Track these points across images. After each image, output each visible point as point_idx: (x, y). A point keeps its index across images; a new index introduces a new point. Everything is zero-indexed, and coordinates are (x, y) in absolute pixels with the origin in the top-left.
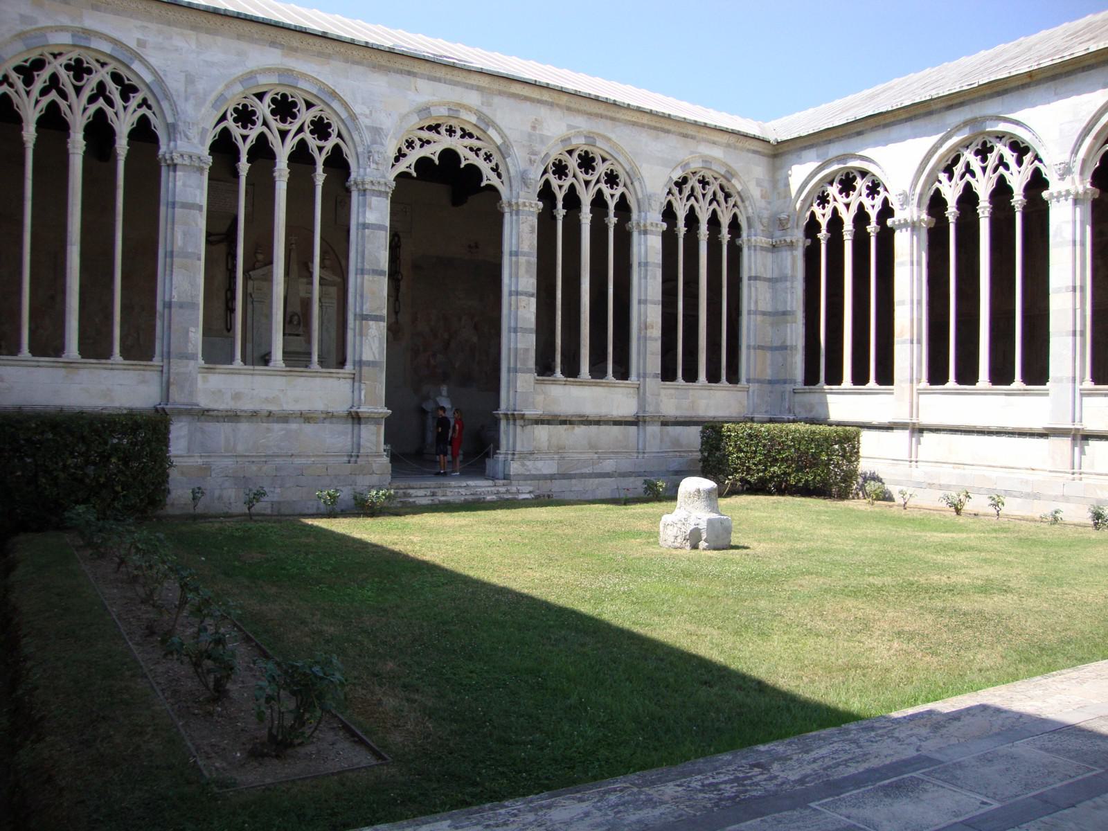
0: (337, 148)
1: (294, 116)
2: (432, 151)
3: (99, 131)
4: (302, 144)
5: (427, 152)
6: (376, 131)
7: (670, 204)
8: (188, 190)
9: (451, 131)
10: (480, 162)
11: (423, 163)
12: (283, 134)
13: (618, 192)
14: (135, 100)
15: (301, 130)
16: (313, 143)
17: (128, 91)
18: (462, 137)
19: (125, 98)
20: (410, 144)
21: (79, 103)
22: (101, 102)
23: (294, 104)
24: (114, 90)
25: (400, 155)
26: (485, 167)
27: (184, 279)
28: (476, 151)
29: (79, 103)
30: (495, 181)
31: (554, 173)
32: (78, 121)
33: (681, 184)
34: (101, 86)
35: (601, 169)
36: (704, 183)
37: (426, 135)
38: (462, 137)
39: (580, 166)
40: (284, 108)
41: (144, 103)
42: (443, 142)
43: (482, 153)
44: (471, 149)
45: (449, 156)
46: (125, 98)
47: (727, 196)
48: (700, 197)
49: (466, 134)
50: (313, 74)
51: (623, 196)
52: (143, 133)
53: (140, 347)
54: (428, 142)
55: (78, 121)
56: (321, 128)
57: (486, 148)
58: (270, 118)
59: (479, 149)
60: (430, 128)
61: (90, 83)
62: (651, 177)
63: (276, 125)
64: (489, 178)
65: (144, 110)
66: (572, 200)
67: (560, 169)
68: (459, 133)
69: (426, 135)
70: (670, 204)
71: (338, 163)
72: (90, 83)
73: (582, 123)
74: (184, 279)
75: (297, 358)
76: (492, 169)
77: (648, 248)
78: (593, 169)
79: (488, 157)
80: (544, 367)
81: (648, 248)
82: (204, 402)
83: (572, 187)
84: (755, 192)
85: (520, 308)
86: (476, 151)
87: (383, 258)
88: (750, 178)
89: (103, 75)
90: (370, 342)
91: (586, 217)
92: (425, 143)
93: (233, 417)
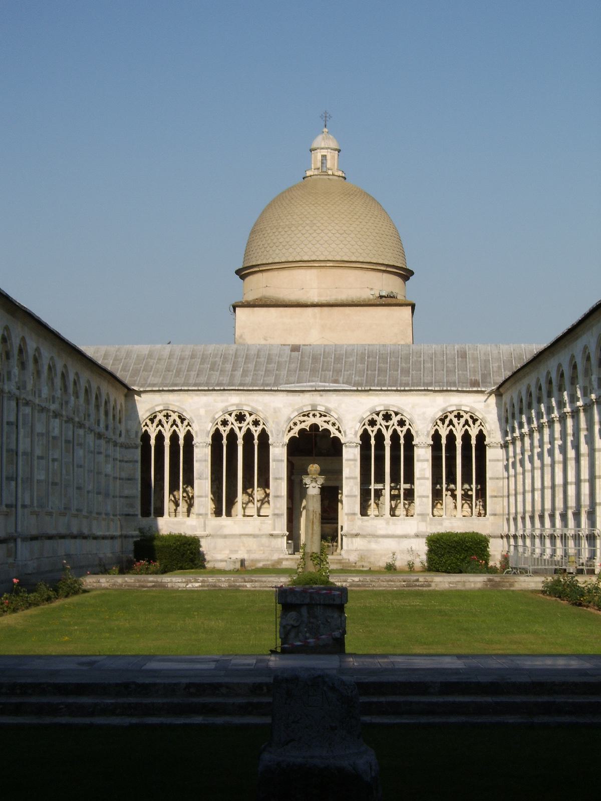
0: (263, 430)
1: (245, 420)
2: (306, 426)
3: (174, 437)
4: (249, 430)
5: (303, 426)
7: (437, 431)
9: (314, 415)
10: (330, 427)
11: (302, 431)
12: (240, 428)
13: (405, 429)
14: (186, 423)
15: (248, 424)
16: (253, 428)
17: (183, 420)
18: (320, 417)
19: (182, 423)
20: (295, 424)
21: (167, 426)
22: (174, 426)
23: (245, 415)
24: (178, 421)
25: (291, 429)
26: (333, 430)
28: (328, 422)
29: (167, 426)
30: (337, 434)
31: (369, 425)
32: (167, 435)
34: (174, 421)
37: (302, 419)
38: (320, 417)
39: (383, 419)
40: (240, 418)
41: (189, 425)
42: (311, 420)
43: (330, 423)
44: (325, 422)
45: (314, 427)
46: (182, 423)
47: (475, 421)
48: (456, 424)
49: (321, 415)
51: (409, 431)
54: (304, 421)
55: (167, 435)
57: (332, 420)
58: (235, 423)
59: (329, 421)
60: (304, 416)
61: (171, 420)
63: (237, 425)
64: (334, 432)
65: (189, 428)
66: (380, 437)
67: (372, 423)
68: (318, 415)
69: (302, 419)
70: (437, 431)
71: (264, 436)
72: (171, 420)
76: (336, 429)
78: (391, 419)
79: (334, 424)
83: (379, 431)
86: (328, 422)
89: (174, 416)
91: (388, 443)
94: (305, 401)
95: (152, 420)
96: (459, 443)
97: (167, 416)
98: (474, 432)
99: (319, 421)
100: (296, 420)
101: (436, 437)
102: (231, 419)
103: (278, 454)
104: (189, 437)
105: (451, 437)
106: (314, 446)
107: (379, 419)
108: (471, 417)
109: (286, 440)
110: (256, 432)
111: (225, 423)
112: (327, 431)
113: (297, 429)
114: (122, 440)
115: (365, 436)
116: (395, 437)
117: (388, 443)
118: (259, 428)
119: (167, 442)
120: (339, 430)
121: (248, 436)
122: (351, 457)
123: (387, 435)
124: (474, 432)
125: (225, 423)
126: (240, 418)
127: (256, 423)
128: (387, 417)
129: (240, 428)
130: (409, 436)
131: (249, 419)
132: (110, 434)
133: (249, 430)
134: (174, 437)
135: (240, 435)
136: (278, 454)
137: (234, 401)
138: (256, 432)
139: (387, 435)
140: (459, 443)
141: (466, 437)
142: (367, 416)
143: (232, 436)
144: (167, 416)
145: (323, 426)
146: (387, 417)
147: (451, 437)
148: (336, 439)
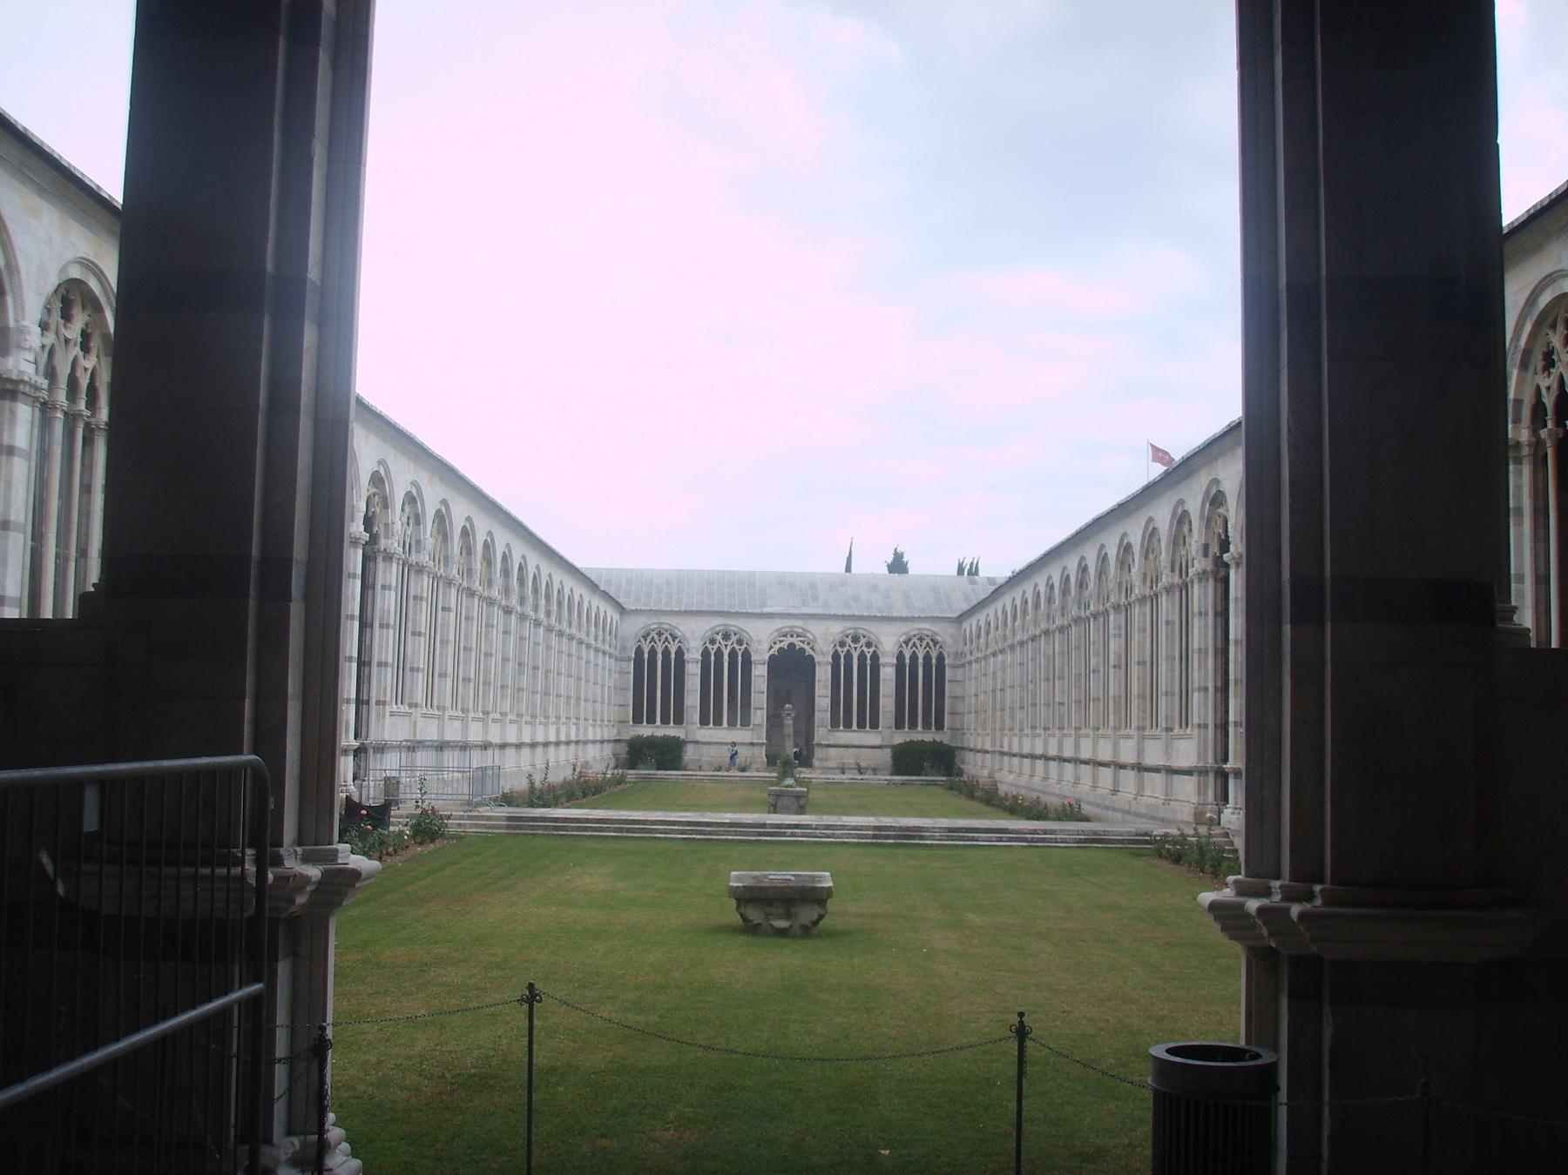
2: (784, 645)
3: (666, 652)
6: (759, 642)
8: (693, 671)
11: (780, 650)
27: (692, 699)
33: (906, 643)
35: (863, 641)
36: (921, 639)
40: (726, 637)
45: (792, 645)
50: (735, 624)
52: (680, 652)
53: (679, 720)
56: (740, 642)
62: (889, 641)
64: (809, 651)
66: (848, 656)
67: (842, 644)
73: (850, 624)
74: (692, 699)
75: (732, 723)
77: (888, 673)
81: (888, 673)
82: (699, 738)
84: (949, 640)
85: (823, 701)
87: (764, 687)
88: (944, 633)
90: (759, 716)
91: (855, 661)
93: (709, 743)
94: (779, 624)
95: (645, 638)
96: (921, 661)
97: (660, 634)
98: (934, 655)
99: (794, 640)
101: (900, 657)
102: (719, 638)
103: (760, 672)
104: (680, 652)
105: (914, 657)
106: (791, 667)
107: (849, 640)
110: (740, 650)
111: (713, 642)
112: (803, 650)
114: (617, 653)
115: (836, 656)
116: (862, 657)
117: (855, 661)
119: (660, 656)
121: (733, 654)
122: (823, 674)
123: (855, 655)
124: (934, 655)
125: (713, 642)
126: (726, 637)
127: (740, 642)
128: (856, 639)
130: (875, 657)
131: (734, 638)
132: (607, 647)
134: (666, 652)
136: (760, 672)
137: (717, 622)
138: (740, 650)
139: (855, 655)
140: (921, 661)
141: (927, 658)
142: (838, 638)
143: (719, 654)
144: (660, 634)
145: (799, 645)
146: (856, 639)
147: (914, 657)
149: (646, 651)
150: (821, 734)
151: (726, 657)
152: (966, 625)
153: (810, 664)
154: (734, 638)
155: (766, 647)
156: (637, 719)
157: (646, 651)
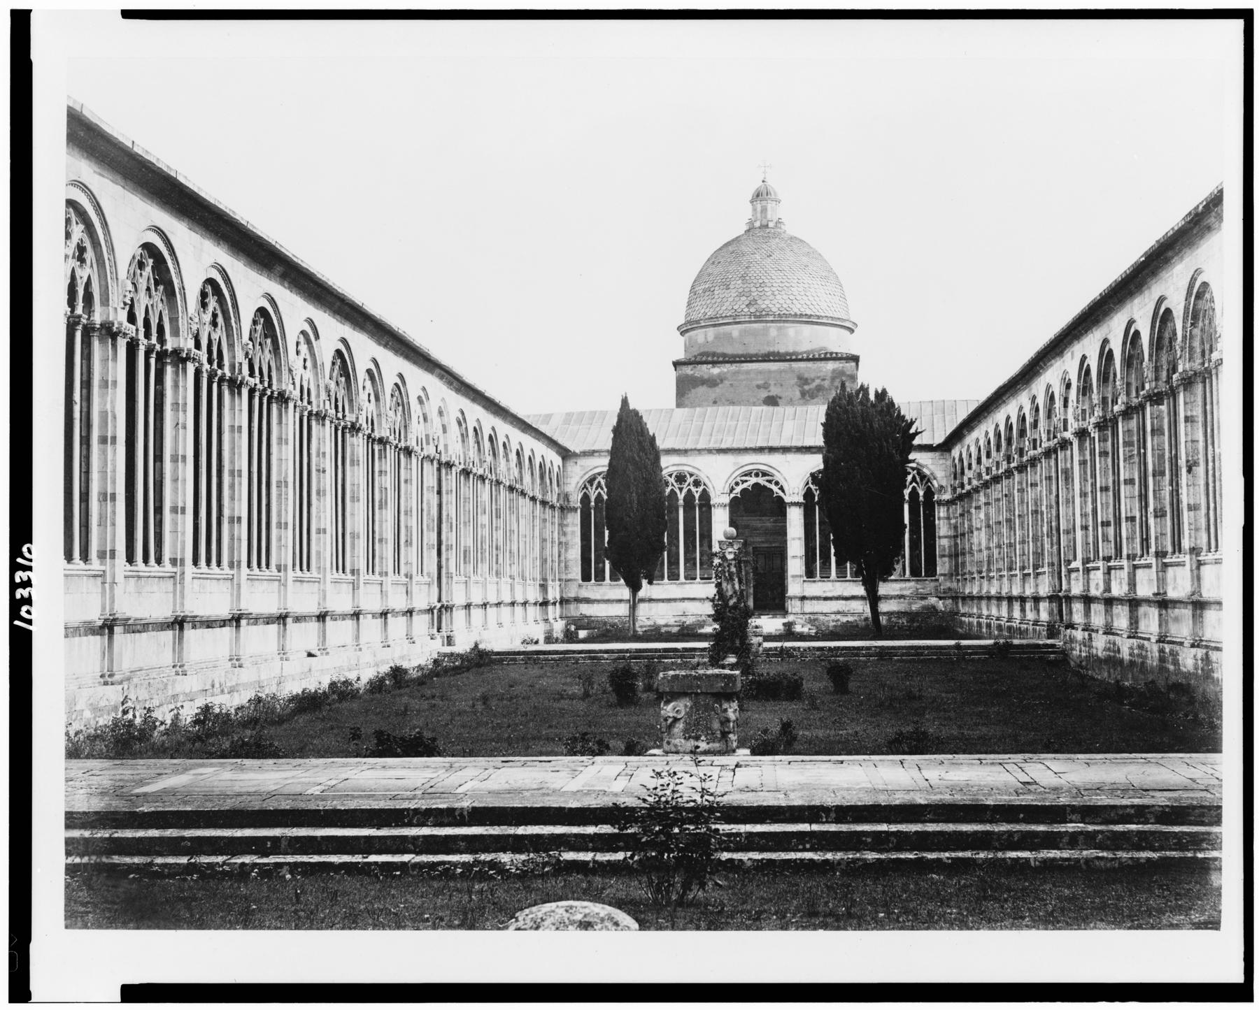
4: (689, 490)
5: (745, 485)
9: (757, 475)
11: (744, 491)
12: (681, 489)
16: (694, 489)
20: (737, 484)
25: (732, 490)
26: (775, 489)
28: (770, 481)
30: (781, 494)
42: (753, 480)
45: (756, 485)
56: (697, 483)
71: (705, 496)
75: (690, 577)
79: (777, 483)
80: (810, 573)
92: (743, 482)
99: (761, 481)
100: (738, 479)
108: (919, 473)
109: (726, 500)
110: (697, 492)
113: (738, 489)
118: (700, 489)
120: (782, 489)
129: (681, 489)
131: (690, 480)
133: (689, 490)
135: (681, 496)
138: (697, 492)
148: (780, 498)
149: (593, 498)
150: (795, 587)
151: (681, 502)
152: (955, 452)
153: (780, 507)
154: (690, 480)
155: (727, 490)
156: (586, 577)
157: (593, 498)
